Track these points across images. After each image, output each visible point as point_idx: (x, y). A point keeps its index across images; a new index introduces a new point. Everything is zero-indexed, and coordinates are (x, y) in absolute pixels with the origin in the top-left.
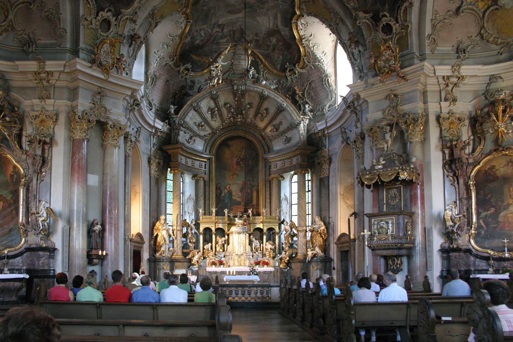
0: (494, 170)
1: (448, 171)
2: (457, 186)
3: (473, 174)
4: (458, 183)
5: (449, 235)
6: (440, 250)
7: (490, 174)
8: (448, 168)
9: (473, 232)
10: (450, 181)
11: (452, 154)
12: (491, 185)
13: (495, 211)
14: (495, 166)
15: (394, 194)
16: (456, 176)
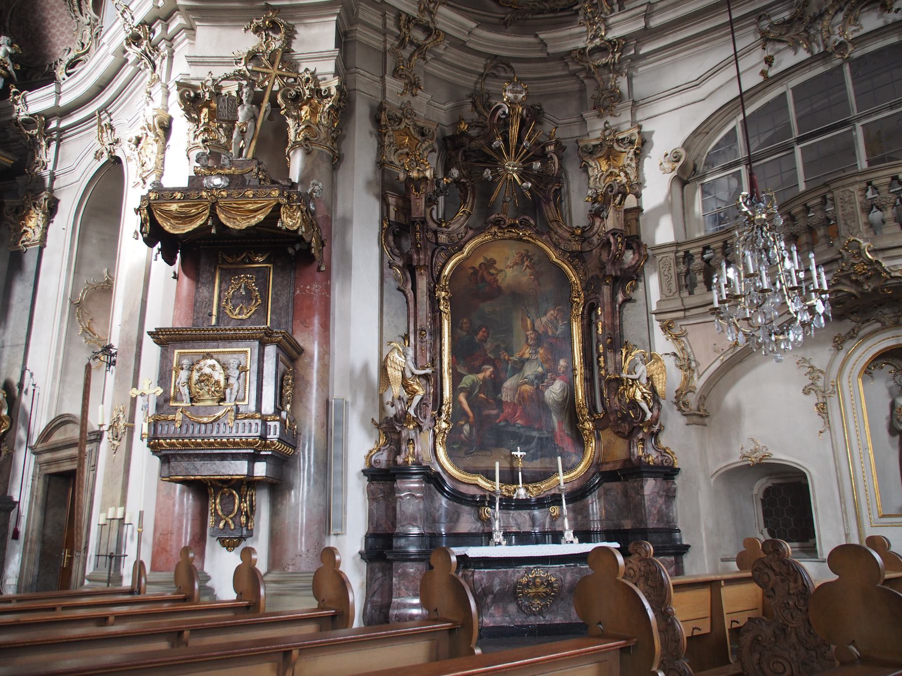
0: (492, 271)
1: (392, 252)
2: (410, 295)
3: (446, 272)
4: (414, 288)
5: (391, 429)
6: (364, 472)
7: (483, 279)
8: (392, 244)
9: (444, 425)
10: (396, 279)
11: (405, 207)
12: (486, 307)
13: (493, 373)
14: (495, 262)
15: (246, 288)
16: (410, 269)
